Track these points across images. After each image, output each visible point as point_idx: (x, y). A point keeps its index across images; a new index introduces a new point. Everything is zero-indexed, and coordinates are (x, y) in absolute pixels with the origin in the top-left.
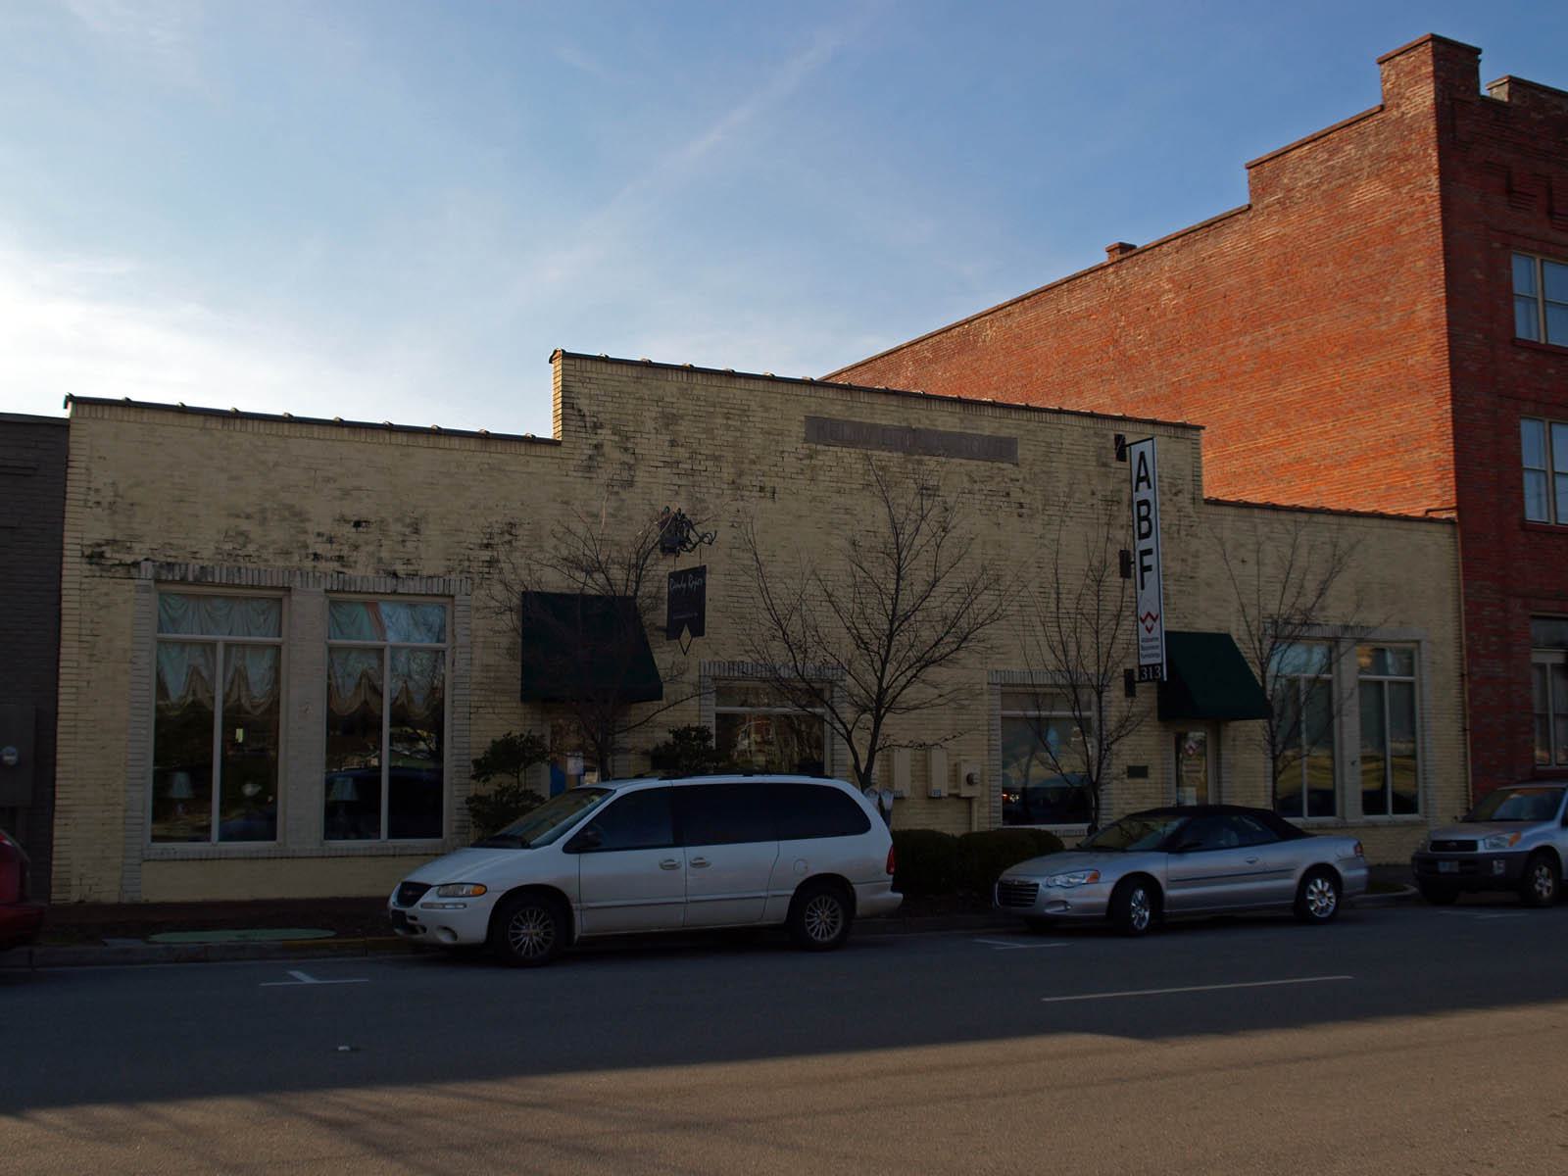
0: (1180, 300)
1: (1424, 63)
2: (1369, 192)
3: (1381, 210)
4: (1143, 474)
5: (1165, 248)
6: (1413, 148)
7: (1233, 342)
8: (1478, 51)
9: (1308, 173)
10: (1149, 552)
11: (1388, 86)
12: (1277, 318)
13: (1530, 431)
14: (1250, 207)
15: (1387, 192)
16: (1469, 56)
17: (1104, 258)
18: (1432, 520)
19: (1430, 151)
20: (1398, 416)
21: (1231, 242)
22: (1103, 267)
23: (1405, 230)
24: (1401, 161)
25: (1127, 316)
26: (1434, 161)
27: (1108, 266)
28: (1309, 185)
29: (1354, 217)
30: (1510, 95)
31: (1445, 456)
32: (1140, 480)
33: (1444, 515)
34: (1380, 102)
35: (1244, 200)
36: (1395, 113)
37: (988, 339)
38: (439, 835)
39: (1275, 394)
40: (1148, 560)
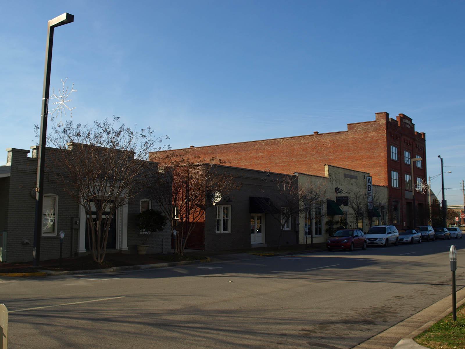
0: (331, 144)
1: (384, 116)
2: (372, 134)
3: (375, 137)
4: (369, 181)
5: (328, 135)
6: (382, 128)
7: (344, 153)
8: (389, 114)
9: (360, 128)
10: (370, 193)
11: (377, 118)
12: (353, 151)
13: (417, 178)
14: (348, 131)
15: (376, 134)
16: (387, 114)
17: (313, 134)
18: (384, 187)
19: (385, 130)
20: (377, 170)
21: (343, 137)
22: (313, 135)
23: (380, 141)
24: (379, 130)
25: (318, 145)
26: (385, 131)
27: (314, 135)
28: (360, 130)
29: (369, 137)
30: (391, 121)
31: (385, 177)
32: (368, 182)
33: (386, 186)
34: (375, 120)
35: (347, 130)
36: (378, 122)
37: (281, 144)
38: (321, 234)
39: (352, 163)
40: (370, 194)
